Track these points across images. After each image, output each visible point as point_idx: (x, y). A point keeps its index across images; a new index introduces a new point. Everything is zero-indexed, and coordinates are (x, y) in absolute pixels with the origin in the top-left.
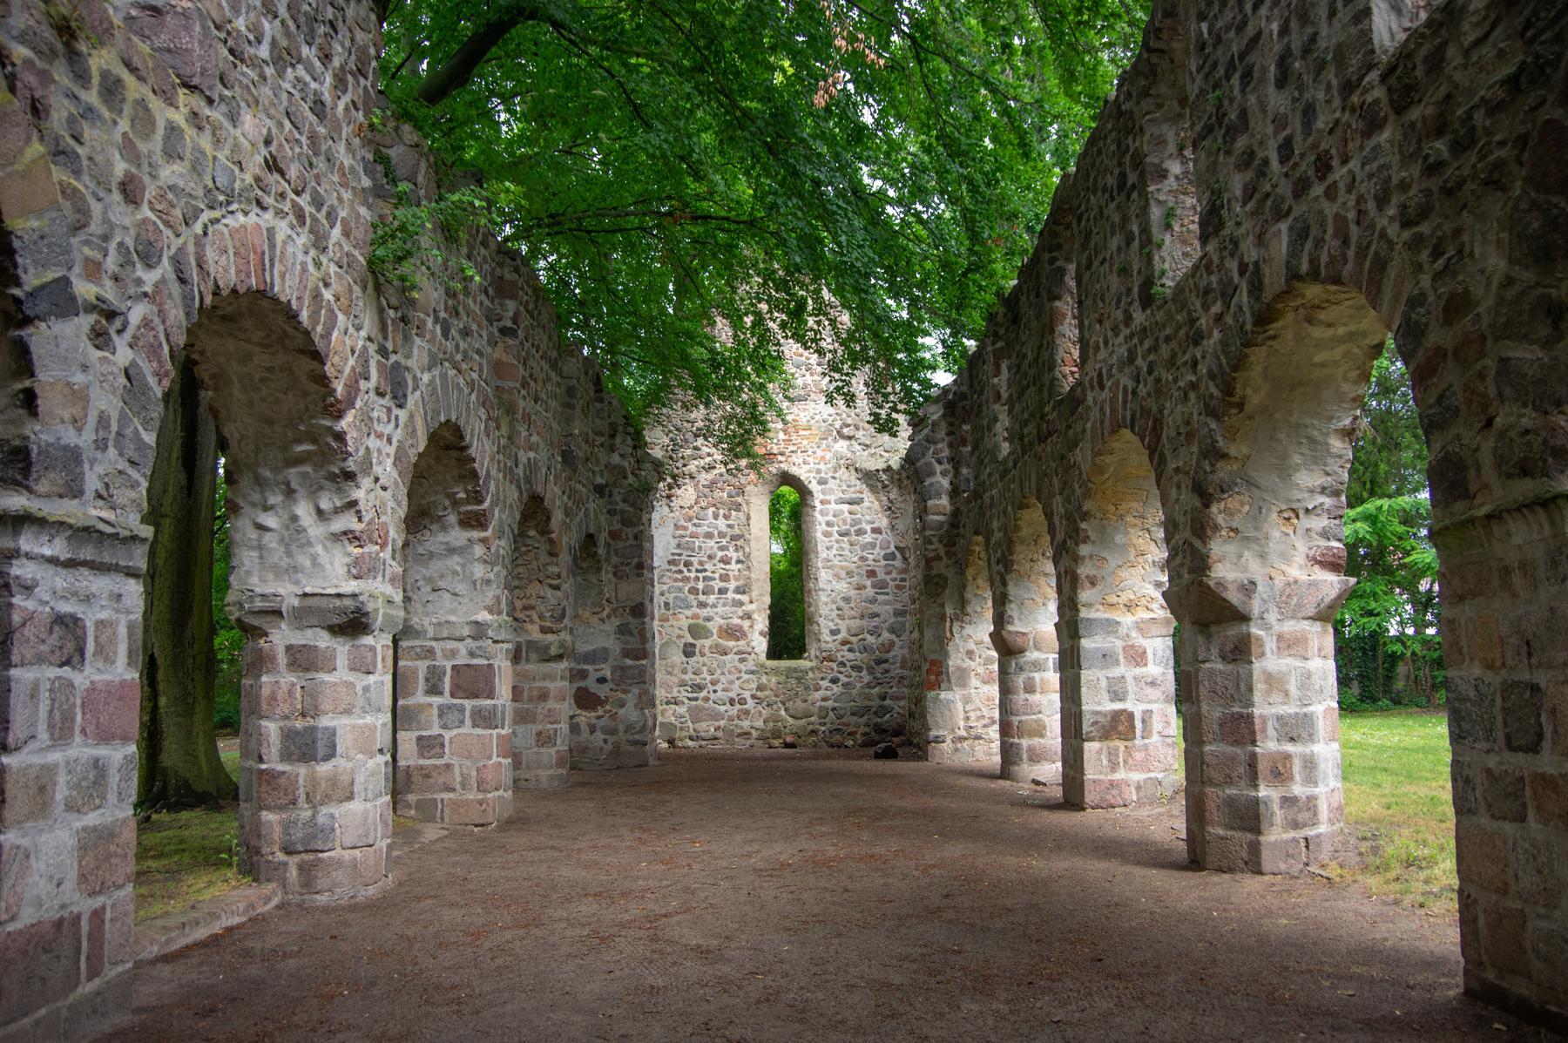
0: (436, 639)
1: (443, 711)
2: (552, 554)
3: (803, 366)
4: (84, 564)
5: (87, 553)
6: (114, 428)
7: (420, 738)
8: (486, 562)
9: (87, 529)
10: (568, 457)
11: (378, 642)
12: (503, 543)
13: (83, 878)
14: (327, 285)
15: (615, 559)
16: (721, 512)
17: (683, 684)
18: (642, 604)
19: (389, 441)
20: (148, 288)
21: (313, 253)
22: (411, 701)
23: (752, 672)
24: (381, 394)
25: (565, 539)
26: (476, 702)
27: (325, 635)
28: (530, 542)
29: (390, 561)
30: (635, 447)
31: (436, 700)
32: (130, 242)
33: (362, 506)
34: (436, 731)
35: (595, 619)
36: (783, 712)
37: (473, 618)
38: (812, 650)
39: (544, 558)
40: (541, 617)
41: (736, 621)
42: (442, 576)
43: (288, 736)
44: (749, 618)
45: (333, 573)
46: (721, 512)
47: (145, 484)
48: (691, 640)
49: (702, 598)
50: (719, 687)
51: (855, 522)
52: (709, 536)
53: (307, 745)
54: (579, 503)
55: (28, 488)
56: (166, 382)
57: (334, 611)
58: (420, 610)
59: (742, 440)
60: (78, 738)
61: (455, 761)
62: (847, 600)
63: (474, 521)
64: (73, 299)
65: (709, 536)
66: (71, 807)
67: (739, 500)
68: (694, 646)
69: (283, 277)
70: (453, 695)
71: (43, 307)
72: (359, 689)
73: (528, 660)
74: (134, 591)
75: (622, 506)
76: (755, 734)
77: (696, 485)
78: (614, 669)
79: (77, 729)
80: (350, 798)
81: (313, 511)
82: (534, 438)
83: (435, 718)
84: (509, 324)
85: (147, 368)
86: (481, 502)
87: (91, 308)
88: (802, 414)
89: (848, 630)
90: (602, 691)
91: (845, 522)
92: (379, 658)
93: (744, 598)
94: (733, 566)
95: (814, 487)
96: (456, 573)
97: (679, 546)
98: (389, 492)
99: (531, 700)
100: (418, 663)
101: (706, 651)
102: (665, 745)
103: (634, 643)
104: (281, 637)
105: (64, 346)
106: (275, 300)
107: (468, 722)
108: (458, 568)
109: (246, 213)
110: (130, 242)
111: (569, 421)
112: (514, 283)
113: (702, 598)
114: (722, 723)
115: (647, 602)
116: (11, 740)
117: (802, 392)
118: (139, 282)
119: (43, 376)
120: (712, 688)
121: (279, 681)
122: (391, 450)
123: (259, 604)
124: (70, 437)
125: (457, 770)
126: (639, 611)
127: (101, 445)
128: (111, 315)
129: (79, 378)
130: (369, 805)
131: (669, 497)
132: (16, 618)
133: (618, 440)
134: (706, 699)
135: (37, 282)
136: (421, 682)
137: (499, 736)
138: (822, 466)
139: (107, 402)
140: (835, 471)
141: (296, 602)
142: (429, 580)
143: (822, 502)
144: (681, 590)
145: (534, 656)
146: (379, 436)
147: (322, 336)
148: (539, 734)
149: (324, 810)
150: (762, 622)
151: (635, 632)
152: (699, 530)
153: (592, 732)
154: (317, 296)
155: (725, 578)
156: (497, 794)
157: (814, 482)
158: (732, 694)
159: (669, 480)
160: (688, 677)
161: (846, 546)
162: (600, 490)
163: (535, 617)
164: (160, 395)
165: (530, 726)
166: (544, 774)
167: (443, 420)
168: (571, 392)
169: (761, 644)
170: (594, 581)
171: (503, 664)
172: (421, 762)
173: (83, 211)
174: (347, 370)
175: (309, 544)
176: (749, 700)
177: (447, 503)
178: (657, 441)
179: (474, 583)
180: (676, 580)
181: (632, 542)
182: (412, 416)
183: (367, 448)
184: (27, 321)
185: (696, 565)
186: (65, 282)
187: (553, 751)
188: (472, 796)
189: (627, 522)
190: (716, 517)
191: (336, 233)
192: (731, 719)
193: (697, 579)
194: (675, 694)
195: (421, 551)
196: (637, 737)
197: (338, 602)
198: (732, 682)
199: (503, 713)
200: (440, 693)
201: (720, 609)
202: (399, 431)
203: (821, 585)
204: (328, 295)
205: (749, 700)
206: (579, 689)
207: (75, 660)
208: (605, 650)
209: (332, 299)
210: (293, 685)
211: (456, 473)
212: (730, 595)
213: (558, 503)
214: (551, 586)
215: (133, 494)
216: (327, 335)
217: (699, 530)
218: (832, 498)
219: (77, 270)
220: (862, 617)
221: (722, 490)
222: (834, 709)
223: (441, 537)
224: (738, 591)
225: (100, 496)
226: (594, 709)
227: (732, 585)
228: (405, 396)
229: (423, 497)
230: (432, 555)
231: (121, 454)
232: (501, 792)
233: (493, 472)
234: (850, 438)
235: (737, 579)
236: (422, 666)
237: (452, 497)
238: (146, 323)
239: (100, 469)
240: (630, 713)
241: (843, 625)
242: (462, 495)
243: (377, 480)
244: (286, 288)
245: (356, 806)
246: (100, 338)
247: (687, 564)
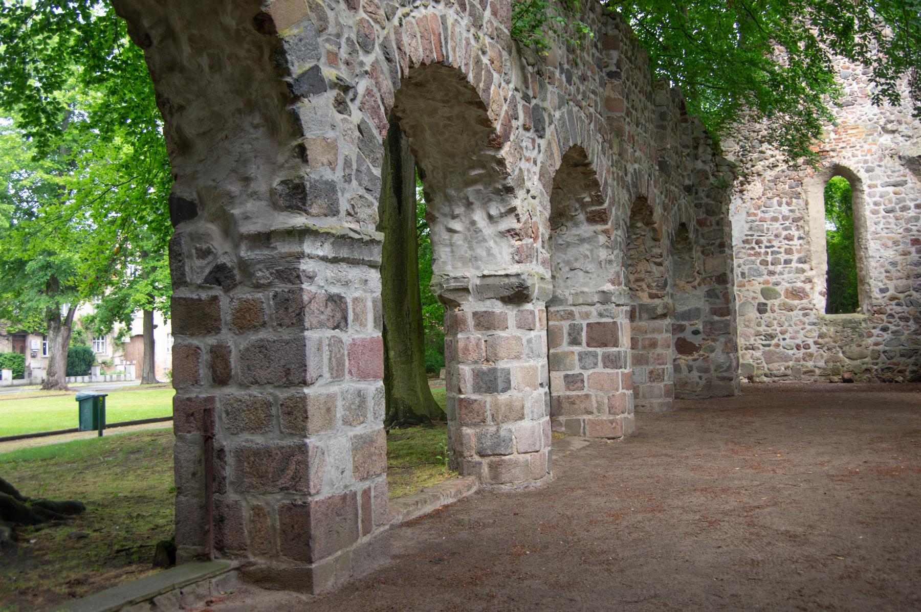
0: (574, 305)
1: (582, 357)
2: (655, 240)
3: (850, 77)
4: (343, 260)
5: (344, 253)
6: (355, 167)
7: (566, 376)
8: (608, 247)
9: (343, 237)
10: (663, 166)
11: (536, 307)
12: (619, 233)
13: (356, 469)
14: (484, 53)
15: (702, 241)
16: (784, 200)
17: (758, 334)
18: (725, 274)
19: (535, 163)
20: (368, 68)
21: (473, 30)
22: (559, 350)
23: (814, 324)
24: (527, 129)
25: (664, 228)
26: (605, 350)
27: (499, 304)
28: (638, 231)
29: (541, 250)
30: (714, 155)
31: (576, 349)
32: (353, 37)
33: (519, 211)
34: (577, 371)
35: (689, 287)
36: (841, 355)
37: (599, 289)
38: (865, 305)
39: (650, 243)
40: (649, 287)
41: (799, 284)
42: (576, 259)
43: (478, 375)
44: (810, 281)
45: (501, 260)
46: (784, 200)
47: (376, 204)
48: (764, 301)
49: (771, 268)
50: (787, 336)
51: (899, 201)
52: (775, 219)
53: (490, 382)
54: (674, 200)
55: (306, 211)
56: (385, 133)
57: (505, 287)
58: (562, 284)
59: (799, 144)
60: (347, 376)
61: (592, 392)
62: (894, 264)
63: (598, 218)
64: (322, 80)
65: (775, 219)
66: (346, 422)
67: (799, 189)
68: (765, 304)
69: (454, 50)
70: (588, 345)
71: (305, 88)
72: (524, 341)
73: (640, 319)
74: (374, 277)
75: (705, 200)
76: (817, 371)
77: (763, 181)
78: (705, 324)
79: (346, 371)
80: (522, 418)
81: (485, 217)
82: (638, 154)
83: (577, 362)
84: (614, 69)
85: (372, 123)
86: (602, 203)
87: (334, 86)
88: (850, 117)
89: (896, 288)
90: (697, 340)
91: (890, 201)
92: (537, 319)
93: (806, 266)
94: (796, 242)
95: (862, 175)
96: (586, 256)
97: (751, 229)
98: (537, 200)
99: (644, 347)
100: (562, 322)
101: (776, 308)
102: (746, 381)
103: (720, 304)
104: (469, 306)
105: (319, 113)
106: (450, 67)
107: (600, 364)
108: (588, 253)
109: (426, 7)
110: (353, 37)
111: (662, 138)
112: (615, 37)
113: (771, 268)
114: (791, 363)
115: (728, 272)
116: (308, 378)
117: (850, 99)
118: (362, 64)
119: (309, 135)
120: (781, 337)
121: (469, 338)
122: (537, 169)
123: (453, 284)
124: (328, 175)
125: (593, 399)
126: (723, 279)
127: (347, 179)
128: (346, 89)
129: (331, 134)
130: (535, 423)
131: (741, 191)
132: (306, 298)
133: (700, 150)
134: (777, 345)
135: (300, 72)
136: (566, 336)
137: (623, 374)
138: (869, 157)
139: (348, 149)
140: (881, 160)
141: (478, 282)
142: (568, 263)
143: (869, 187)
144: (753, 262)
145: (645, 316)
146: (528, 160)
147: (484, 91)
148: (651, 372)
149: (505, 426)
150: (821, 284)
151: (721, 295)
152: (767, 215)
153: (690, 371)
154: (478, 62)
155: (789, 251)
156: (623, 416)
157: (862, 171)
158: (798, 341)
159: (741, 178)
160: (762, 329)
161: (892, 220)
162: (688, 189)
163: (645, 287)
164: (381, 142)
165: (644, 367)
166: (656, 402)
167: (571, 144)
168: (663, 116)
169: (821, 302)
170: (687, 258)
171: (623, 321)
172: (568, 393)
173: (323, 19)
174: (503, 114)
175: (484, 240)
176: (812, 345)
177: (577, 206)
178: (731, 149)
179: (600, 263)
180: (750, 255)
181: (715, 227)
182: (549, 143)
183: (520, 169)
184: (297, 98)
185: (765, 243)
186: (316, 69)
187: (662, 385)
188: (605, 417)
189: (710, 212)
190: (780, 205)
191: (487, 13)
192: (798, 360)
193: (767, 253)
194: (752, 342)
195: (560, 242)
196: (725, 374)
197: (506, 280)
198: (797, 332)
199: (625, 357)
200: (580, 344)
201: (786, 276)
202: (541, 155)
203: (871, 253)
204: (485, 60)
205: (812, 345)
206: (678, 339)
207: (342, 324)
208: (698, 309)
209: (488, 62)
210: (479, 339)
211: (582, 183)
212: (794, 265)
213: (658, 201)
214: (655, 263)
215: (369, 211)
216: (487, 89)
217: (767, 215)
218: (879, 182)
219: (323, 60)
220: (908, 277)
221: (784, 183)
222: (884, 352)
223: (575, 231)
224: (800, 261)
225: (349, 214)
226: (691, 354)
227: (795, 257)
228: (544, 129)
229: (560, 203)
230: (568, 245)
231: (360, 185)
232: (626, 415)
233: (610, 181)
234: (893, 132)
235: (799, 252)
236: (565, 325)
237: (580, 201)
238: (369, 92)
239: (348, 195)
240: (718, 356)
241: (891, 285)
242: (588, 199)
243: (528, 191)
244: (457, 59)
245: (526, 424)
246: (341, 106)
247: (758, 242)
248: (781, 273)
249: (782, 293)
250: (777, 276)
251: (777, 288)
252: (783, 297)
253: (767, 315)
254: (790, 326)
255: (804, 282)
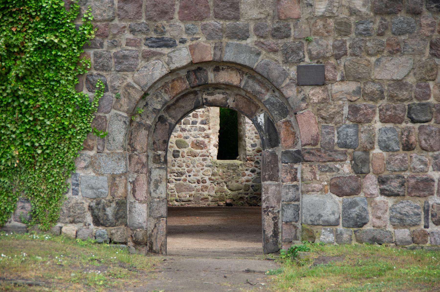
23: (209, 166)
41: (201, 139)
44: (208, 137)
48: (177, 149)
68: (178, 151)
101: (185, 154)
120: (188, 174)
150: (215, 140)
160: (175, 168)
169: (214, 151)
198: (198, 171)
201: (192, 133)
212: (198, 125)
227: (199, 120)
248: (189, 131)
249: (190, 144)
250: (187, 132)
251: (187, 141)
252: (190, 147)
253: (179, 159)
254: (194, 167)
255: (204, 137)
